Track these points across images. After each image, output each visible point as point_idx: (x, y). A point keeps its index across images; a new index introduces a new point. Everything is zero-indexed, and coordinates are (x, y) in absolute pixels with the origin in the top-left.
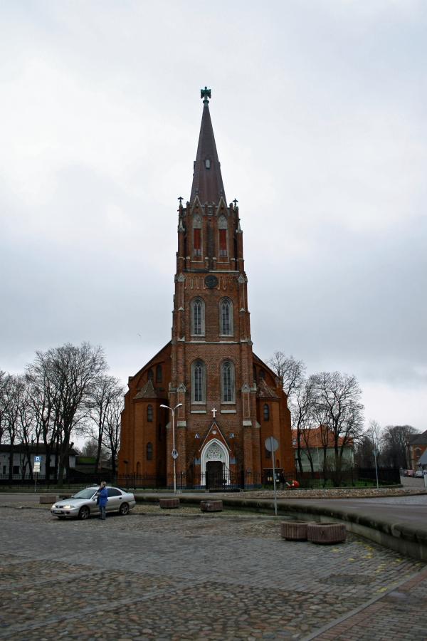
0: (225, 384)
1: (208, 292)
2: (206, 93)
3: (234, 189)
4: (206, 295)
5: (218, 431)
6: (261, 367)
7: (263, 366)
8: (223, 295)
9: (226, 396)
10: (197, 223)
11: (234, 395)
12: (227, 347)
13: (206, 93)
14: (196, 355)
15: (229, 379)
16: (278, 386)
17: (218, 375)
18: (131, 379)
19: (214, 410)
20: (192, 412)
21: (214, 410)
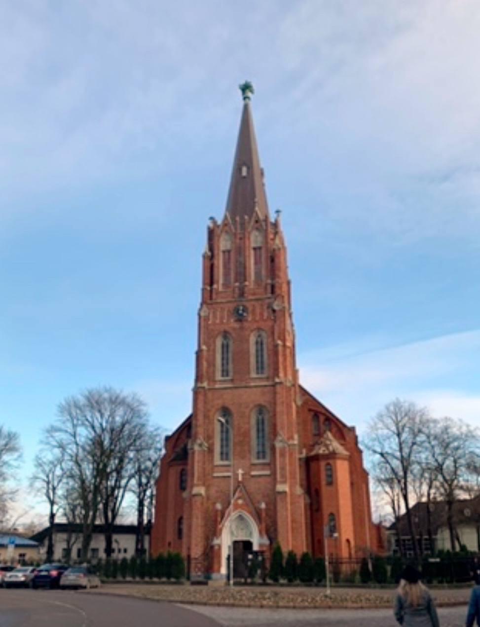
0: (258, 437)
1: (237, 325)
2: (246, 88)
3: (277, 197)
4: (234, 329)
5: (245, 500)
6: (324, 414)
7: (328, 414)
8: (255, 326)
9: (258, 453)
10: (224, 243)
11: (268, 451)
12: (259, 389)
13: (246, 88)
14: (219, 403)
15: (263, 430)
16: (348, 439)
17: (247, 426)
18: (168, 439)
19: (240, 472)
20: (215, 475)
21: (240, 472)
